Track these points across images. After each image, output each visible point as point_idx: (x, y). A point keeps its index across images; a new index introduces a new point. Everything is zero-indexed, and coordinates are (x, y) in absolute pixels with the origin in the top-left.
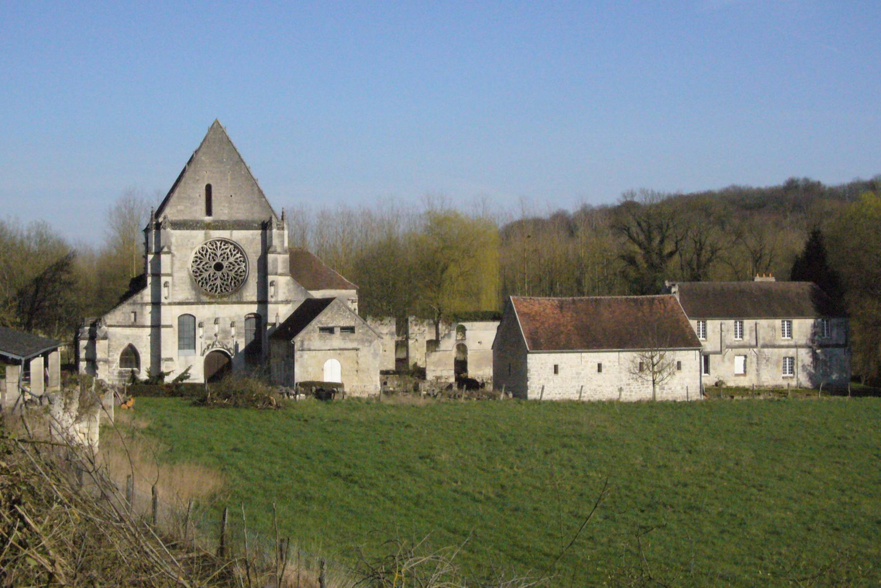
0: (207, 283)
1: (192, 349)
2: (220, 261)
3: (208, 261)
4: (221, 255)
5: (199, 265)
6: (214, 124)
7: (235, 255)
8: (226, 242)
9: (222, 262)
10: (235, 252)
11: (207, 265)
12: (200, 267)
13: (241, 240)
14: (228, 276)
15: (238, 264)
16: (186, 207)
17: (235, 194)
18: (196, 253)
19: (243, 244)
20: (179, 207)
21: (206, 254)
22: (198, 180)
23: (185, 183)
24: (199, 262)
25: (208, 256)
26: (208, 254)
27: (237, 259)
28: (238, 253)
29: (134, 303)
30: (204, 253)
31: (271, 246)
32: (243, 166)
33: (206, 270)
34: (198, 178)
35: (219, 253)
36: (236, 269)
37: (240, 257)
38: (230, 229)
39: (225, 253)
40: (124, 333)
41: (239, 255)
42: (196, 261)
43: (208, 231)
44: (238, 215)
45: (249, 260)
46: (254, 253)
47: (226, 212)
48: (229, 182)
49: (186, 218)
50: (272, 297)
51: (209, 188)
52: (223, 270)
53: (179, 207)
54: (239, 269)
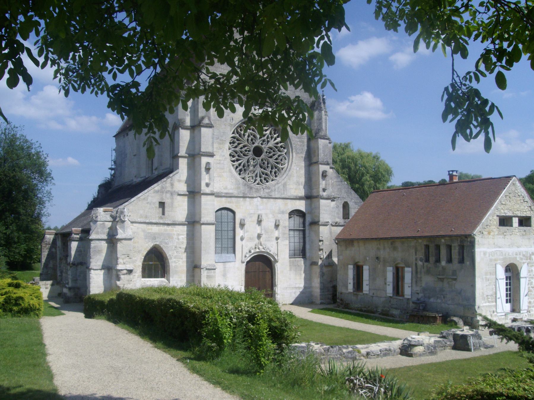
1: (231, 253)
3: (246, 143)
5: (236, 147)
7: (275, 139)
9: (263, 146)
10: (275, 136)
11: (246, 148)
12: (238, 149)
15: (279, 151)
18: (233, 133)
21: (244, 135)
24: (236, 144)
25: (246, 137)
26: (247, 134)
27: (277, 143)
28: (278, 137)
29: (161, 191)
30: (242, 132)
31: (319, 130)
33: (244, 155)
36: (276, 157)
40: (150, 231)
41: (279, 139)
42: (234, 143)
45: (293, 145)
50: (324, 190)
52: (263, 156)
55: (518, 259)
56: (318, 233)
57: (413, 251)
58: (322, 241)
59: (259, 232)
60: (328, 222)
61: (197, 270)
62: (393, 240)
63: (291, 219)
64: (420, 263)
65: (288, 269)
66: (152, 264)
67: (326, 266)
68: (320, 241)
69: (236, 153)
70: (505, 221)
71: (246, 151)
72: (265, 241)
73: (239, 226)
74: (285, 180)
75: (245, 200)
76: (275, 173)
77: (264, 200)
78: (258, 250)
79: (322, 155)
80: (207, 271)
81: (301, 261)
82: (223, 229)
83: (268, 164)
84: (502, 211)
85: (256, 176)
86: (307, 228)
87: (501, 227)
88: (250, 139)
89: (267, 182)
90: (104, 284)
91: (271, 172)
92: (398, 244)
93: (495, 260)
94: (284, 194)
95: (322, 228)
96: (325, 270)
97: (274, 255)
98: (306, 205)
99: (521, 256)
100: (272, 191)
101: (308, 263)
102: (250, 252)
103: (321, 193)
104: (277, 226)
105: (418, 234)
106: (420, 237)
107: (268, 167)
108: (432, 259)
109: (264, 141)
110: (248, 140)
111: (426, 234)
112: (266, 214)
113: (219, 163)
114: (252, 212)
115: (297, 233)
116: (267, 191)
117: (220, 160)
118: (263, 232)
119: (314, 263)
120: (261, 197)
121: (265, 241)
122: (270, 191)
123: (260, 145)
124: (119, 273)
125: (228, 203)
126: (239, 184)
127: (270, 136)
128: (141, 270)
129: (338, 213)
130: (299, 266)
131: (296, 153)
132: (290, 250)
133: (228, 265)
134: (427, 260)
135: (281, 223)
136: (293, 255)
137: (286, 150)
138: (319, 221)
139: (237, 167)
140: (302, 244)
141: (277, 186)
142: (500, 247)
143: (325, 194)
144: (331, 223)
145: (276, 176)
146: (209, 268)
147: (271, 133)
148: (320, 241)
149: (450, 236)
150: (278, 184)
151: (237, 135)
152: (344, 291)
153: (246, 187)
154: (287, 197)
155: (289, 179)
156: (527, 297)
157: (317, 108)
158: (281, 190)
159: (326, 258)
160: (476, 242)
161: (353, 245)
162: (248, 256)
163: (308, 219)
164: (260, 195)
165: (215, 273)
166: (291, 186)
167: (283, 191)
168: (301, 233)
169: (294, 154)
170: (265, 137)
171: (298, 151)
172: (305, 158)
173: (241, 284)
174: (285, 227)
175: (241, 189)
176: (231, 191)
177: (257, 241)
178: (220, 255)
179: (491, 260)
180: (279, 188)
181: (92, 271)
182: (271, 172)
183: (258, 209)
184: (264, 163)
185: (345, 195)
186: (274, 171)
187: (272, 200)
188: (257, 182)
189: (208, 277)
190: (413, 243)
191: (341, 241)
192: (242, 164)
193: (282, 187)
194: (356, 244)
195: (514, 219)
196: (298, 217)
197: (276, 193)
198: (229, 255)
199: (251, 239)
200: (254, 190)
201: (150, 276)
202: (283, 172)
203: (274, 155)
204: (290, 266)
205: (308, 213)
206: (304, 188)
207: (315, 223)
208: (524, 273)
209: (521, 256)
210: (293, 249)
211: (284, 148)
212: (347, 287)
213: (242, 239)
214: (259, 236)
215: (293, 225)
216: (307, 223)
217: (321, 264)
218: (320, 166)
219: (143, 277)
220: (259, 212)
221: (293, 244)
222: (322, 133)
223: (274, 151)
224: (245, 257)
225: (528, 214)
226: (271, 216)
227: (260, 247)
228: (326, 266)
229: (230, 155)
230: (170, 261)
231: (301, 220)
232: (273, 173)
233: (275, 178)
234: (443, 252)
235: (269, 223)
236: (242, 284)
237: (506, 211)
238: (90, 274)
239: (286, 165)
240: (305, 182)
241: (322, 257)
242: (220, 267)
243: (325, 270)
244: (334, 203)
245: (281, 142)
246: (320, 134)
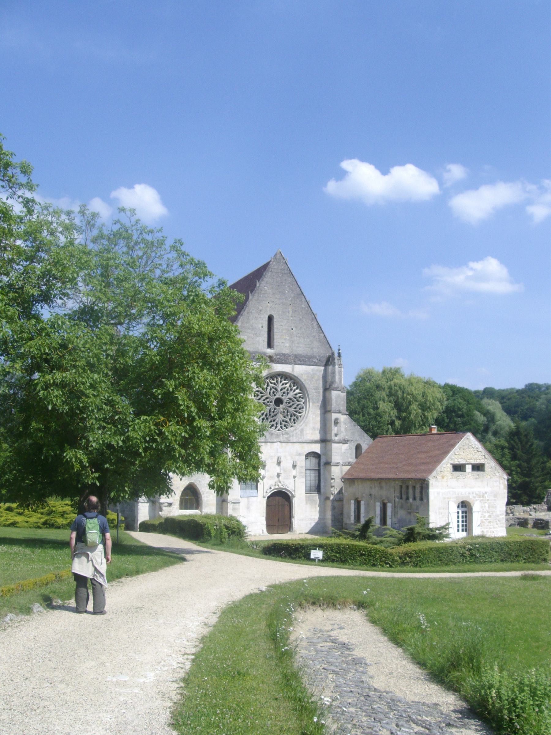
1: (254, 489)
3: (268, 396)
4: (281, 390)
5: (259, 399)
6: (276, 255)
7: (294, 391)
8: (285, 376)
9: (283, 398)
11: (268, 400)
13: (302, 374)
15: (298, 401)
17: (296, 327)
19: (303, 379)
21: (267, 389)
22: (261, 310)
23: (248, 313)
24: (259, 397)
25: (268, 390)
26: (269, 388)
27: (296, 394)
28: (297, 389)
30: (265, 387)
31: (332, 383)
32: (304, 299)
34: (261, 308)
35: (280, 387)
36: (295, 406)
37: (299, 393)
39: (284, 388)
41: (298, 391)
44: (299, 349)
46: (315, 389)
47: (287, 345)
48: (290, 315)
50: (336, 435)
51: (270, 319)
55: (471, 497)
56: (330, 472)
57: (392, 490)
58: (334, 479)
59: (278, 471)
60: (339, 463)
61: (224, 503)
62: (380, 480)
64: (397, 500)
65: (304, 502)
66: (187, 499)
67: (337, 501)
68: (332, 479)
70: (458, 468)
71: (268, 402)
74: (302, 426)
76: (294, 420)
77: (283, 444)
78: (277, 487)
81: (316, 496)
83: (288, 412)
84: (456, 460)
85: (277, 424)
86: (322, 467)
87: (455, 472)
88: (272, 392)
89: (287, 428)
90: (149, 514)
91: (290, 419)
92: (383, 484)
93: (448, 498)
95: (333, 468)
96: (336, 504)
97: (292, 491)
99: (474, 495)
100: (290, 436)
101: (323, 498)
102: (270, 488)
103: (334, 438)
104: (294, 466)
105: (396, 477)
106: (394, 480)
107: (287, 415)
108: (404, 497)
109: (284, 393)
110: (270, 393)
111: (400, 477)
115: (312, 472)
118: (282, 472)
119: (327, 498)
120: (280, 442)
123: (281, 397)
124: (162, 506)
127: (289, 388)
128: (179, 503)
129: (351, 454)
133: (251, 499)
134: (401, 498)
135: (298, 464)
136: (309, 491)
137: (303, 400)
138: (331, 462)
140: (317, 482)
141: (295, 432)
142: (453, 488)
143: (336, 439)
144: (342, 463)
145: (295, 423)
147: (290, 386)
148: (332, 479)
149: (415, 480)
150: (296, 430)
152: (348, 522)
155: (306, 426)
156: (480, 527)
157: (331, 363)
159: (337, 494)
160: (430, 485)
161: (354, 484)
162: (268, 492)
163: (323, 460)
165: (239, 506)
166: (308, 432)
168: (317, 472)
169: (311, 404)
170: (285, 390)
172: (321, 407)
174: (302, 467)
177: (276, 479)
179: (444, 498)
180: (296, 433)
181: (140, 504)
182: (290, 419)
185: (358, 438)
186: (292, 418)
187: (290, 444)
188: (278, 428)
189: (234, 509)
190: (393, 484)
191: (348, 480)
192: (265, 414)
193: (299, 433)
194: (356, 483)
195: (467, 466)
196: (314, 458)
198: (252, 491)
199: (271, 478)
200: (274, 436)
201: (186, 508)
202: (300, 419)
203: (293, 405)
204: (306, 500)
205: (323, 454)
206: (320, 433)
207: (328, 463)
208: (476, 507)
209: (474, 495)
212: (350, 519)
214: (278, 475)
215: (309, 465)
216: (322, 464)
217: (333, 499)
218: (333, 414)
219: (181, 508)
220: (279, 455)
222: (335, 386)
223: (293, 401)
224: (266, 492)
225: (482, 461)
227: (280, 484)
228: (337, 501)
230: (203, 496)
231: (317, 461)
232: (292, 420)
233: (293, 425)
234: (411, 491)
235: (287, 463)
237: (460, 460)
238: (138, 506)
239: (304, 413)
240: (321, 427)
241: (333, 493)
242: (244, 501)
243: (336, 504)
244: (346, 445)
245: (299, 393)
246: (333, 386)
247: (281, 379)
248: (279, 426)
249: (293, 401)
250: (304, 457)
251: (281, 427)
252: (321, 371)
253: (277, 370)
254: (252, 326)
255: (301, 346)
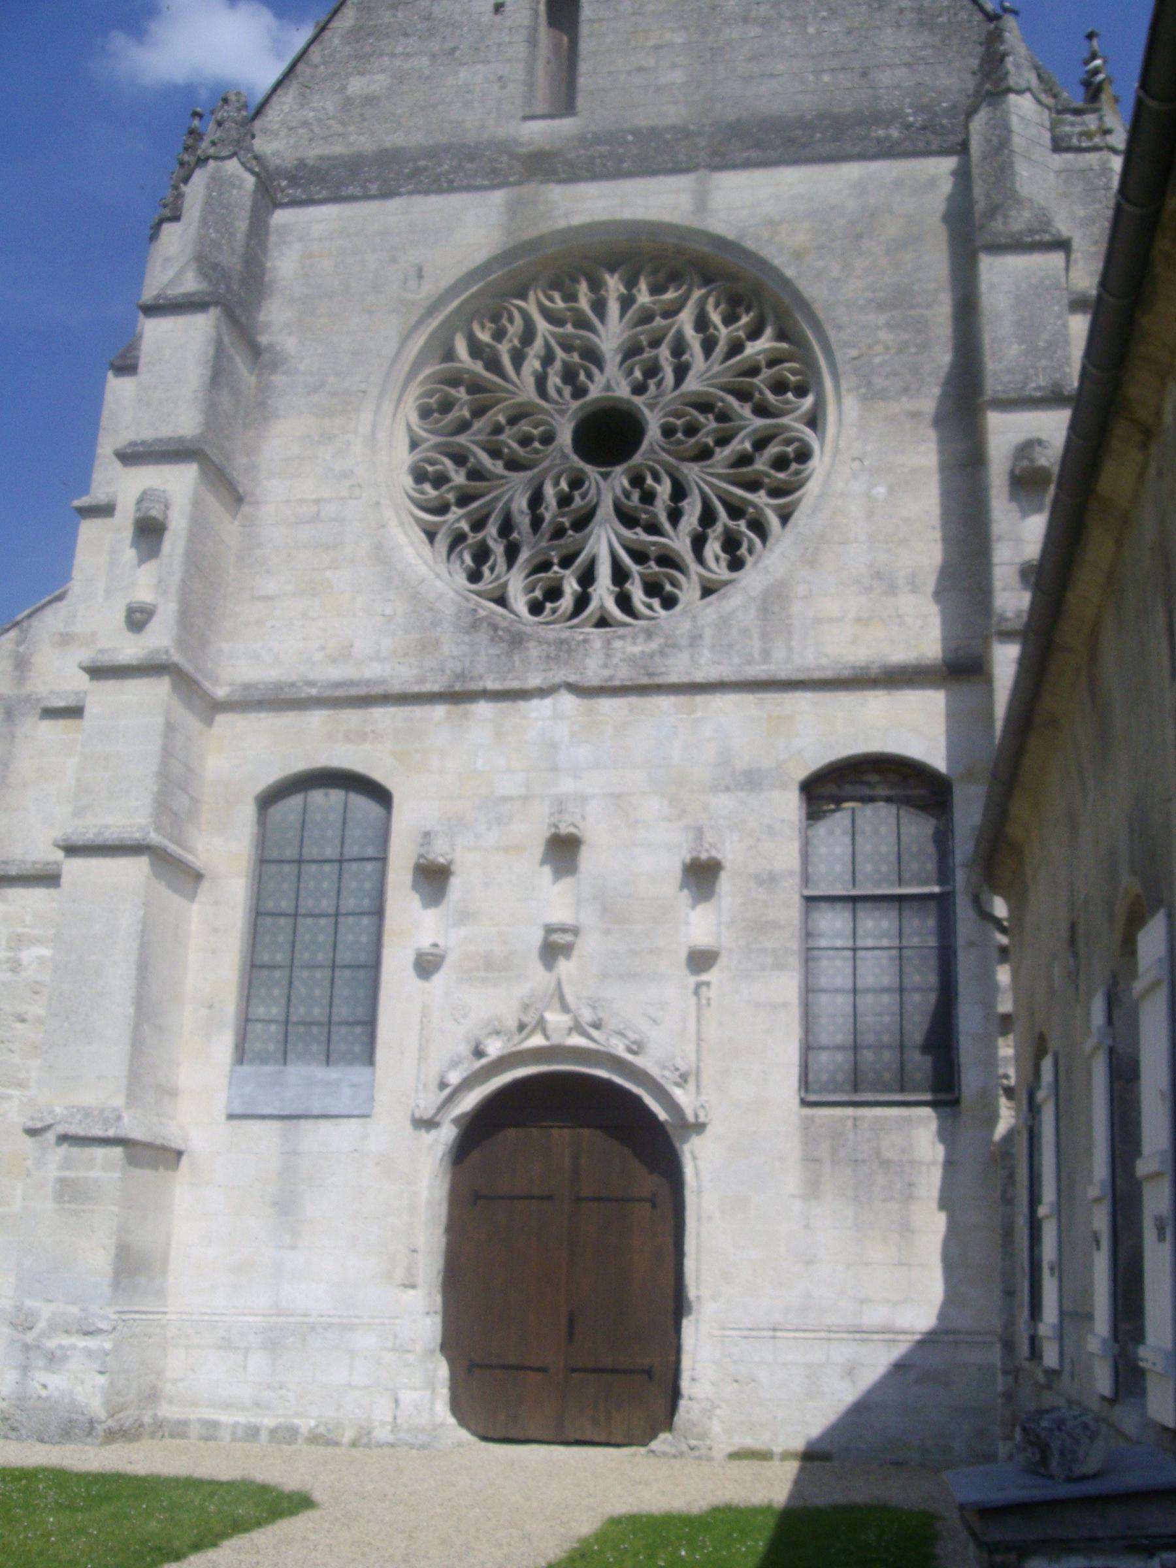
0: (512, 553)
1: (350, 1059)
2: (623, 390)
11: (525, 427)
14: (679, 492)
16: (400, 77)
20: (356, 86)
25: (532, 364)
28: (755, 333)
33: (514, 465)
36: (742, 444)
38: (677, 170)
42: (446, 406)
43: (528, 189)
46: (881, 307)
47: (678, 77)
49: (395, 139)
53: (356, 86)
54: (761, 444)
59: (561, 915)
63: (821, 829)
65: (792, 1180)
69: (460, 459)
72: (604, 976)
73: (408, 878)
75: (466, 716)
77: (607, 705)
78: (537, 1041)
79: (1014, 349)
80: (64, 1149)
82: (308, 904)
94: (766, 655)
98: (954, 719)
107: (675, 516)
112: (618, 799)
113: (315, 519)
114: (509, 785)
116: (637, 649)
117: (318, 501)
121: (604, 976)
122: (654, 645)
125: (348, 738)
126: (435, 624)
130: (885, 1163)
131: (863, 399)
132: (808, 1048)
139: (624, 602)
145: (736, 564)
146: (74, 1129)
147: (702, 323)
151: (478, 367)
153: (483, 637)
154: (783, 675)
158: (745, 632)
164: (572, 679)
166: (830, 607)
167: (757, 644)
171: (879, 382)
173: (399, 1274)
174: (769, 880)
175: (448, 648)
176: (372, 671)
177: (537, 977)
178: (268, 1069)
180: (724, 621)
182: (698, 542)
183: (554, 769)
184: (648, 497)
187: (665, 703)
193: (749, 618)
197: (706, 655)
198: (333, 1073)
200: (534, 651)
204: (810, 1160)
210: (842, 1037)
211: (801, 392)
213: (427, 965)
215: (841, 868)
220: (567, 785)
221: (843, 1002)
226: (653, 807)
227: (554, 1018)
229: (420, 476)
232: (713, 548)
236: (409, 1270)
247: (631, 283)
248: (603, 592)
249: (723, 417)
250: (791, 804)
251: (624, 602)
252: (933, 183)
253: (576, 221)
254: (428, 18)
255: (780, 68)
